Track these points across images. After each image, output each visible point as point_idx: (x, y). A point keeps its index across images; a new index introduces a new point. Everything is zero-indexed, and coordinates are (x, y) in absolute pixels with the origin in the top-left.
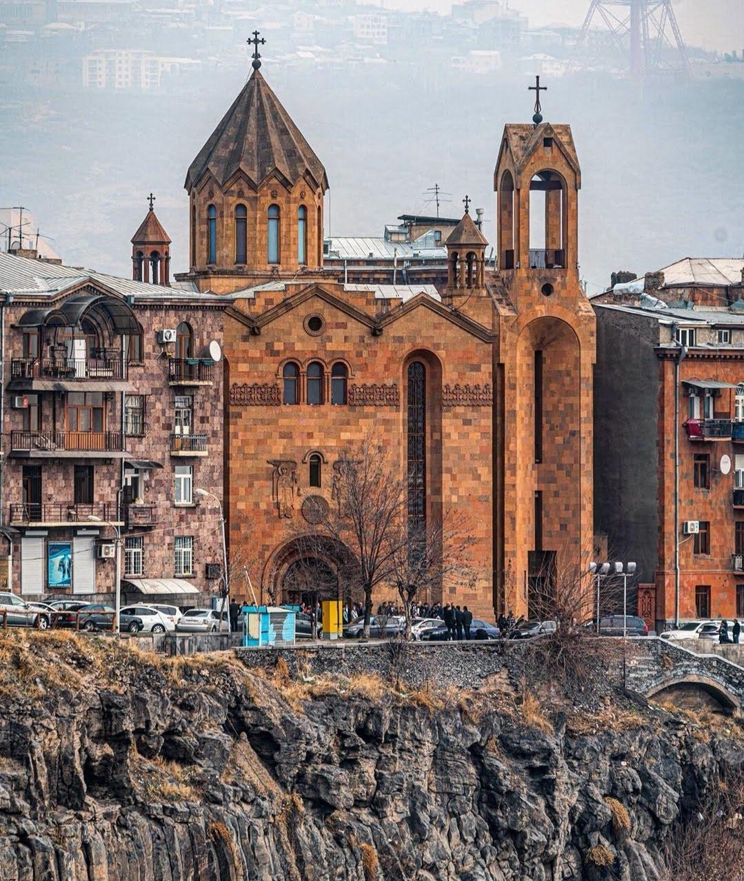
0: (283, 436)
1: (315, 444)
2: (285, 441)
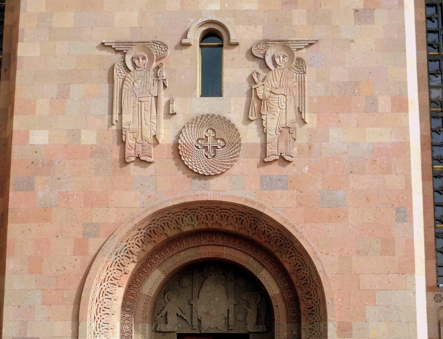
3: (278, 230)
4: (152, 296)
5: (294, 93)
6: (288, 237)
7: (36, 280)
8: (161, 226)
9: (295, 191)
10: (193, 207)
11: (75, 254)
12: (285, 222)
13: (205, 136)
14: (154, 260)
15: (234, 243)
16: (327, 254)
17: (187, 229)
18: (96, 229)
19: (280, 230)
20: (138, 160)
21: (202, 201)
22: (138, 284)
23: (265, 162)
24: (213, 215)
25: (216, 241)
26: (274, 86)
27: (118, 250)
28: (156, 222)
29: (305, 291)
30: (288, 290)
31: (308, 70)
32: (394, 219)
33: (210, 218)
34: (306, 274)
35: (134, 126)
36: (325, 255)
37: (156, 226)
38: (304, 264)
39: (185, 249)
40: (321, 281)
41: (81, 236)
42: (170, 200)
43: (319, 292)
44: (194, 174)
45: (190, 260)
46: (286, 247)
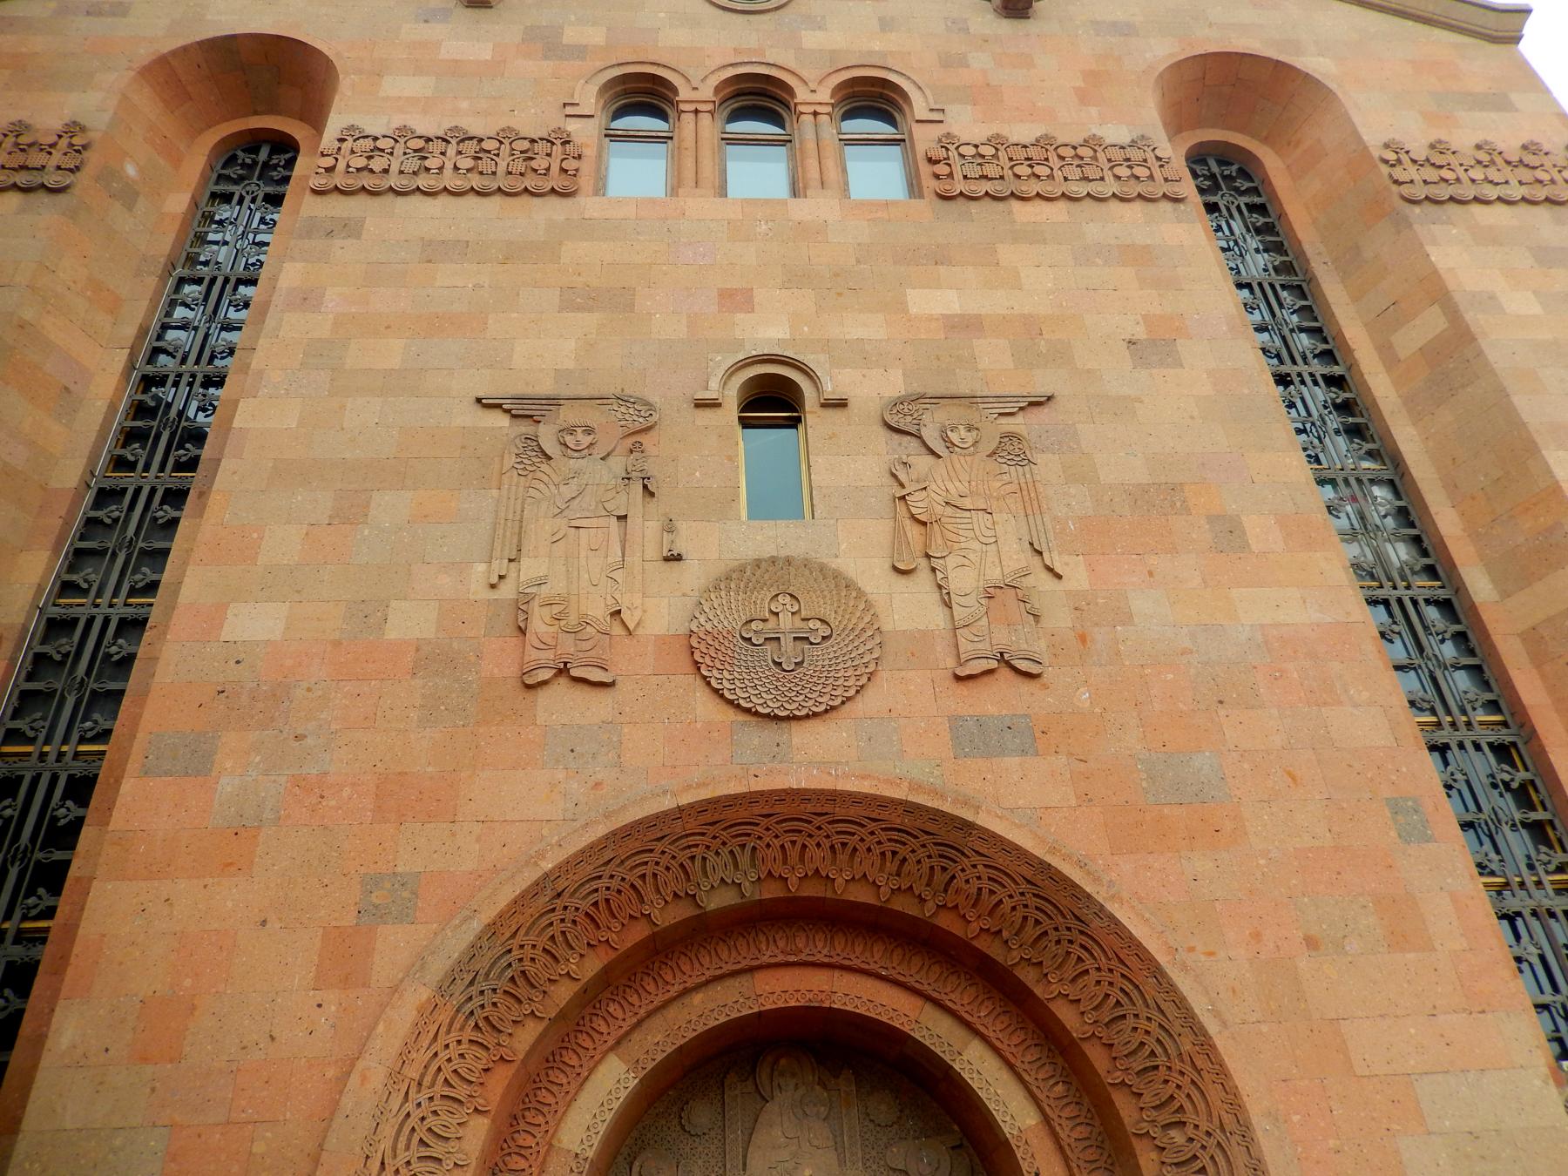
0: (577, 299)
1: (769, 331)
2: (590, 320)
3: (1029, 882)
4: (590, 1154)
5: (1013, 507)
6: (1065, 902)
7: (153, 1090)
8: (632, 886)
9: (1063, 759)
10: (743, 814)
11: (319, 983)
12: (1053, 850)
13: (771, 612)
14: (602, 1022)
15: (868, 954)
16: (1211, 954)
17: (719, 901)
18: (406, 894)
19: (1038, 879)
20: (563, 680)
21: (772, 792)
22: (545, 1110)
23: (958, 678)
24: (804, 846)
25: (807, 951)
26: (953, 491)
27: (482, 964)
28: (620, 872)
29: (1148, 1099)
30: (1068, 1109)
31: (1039, 458)
32: (1393, 834)
33: (793, 854)
34: (1147, 1032)
35: (556, 587)
36: (1203, 958)
37: (615, 884)
38: (1135, 994)
39: (707, 982)
40: (1213, 1047)
41: (349, 920)
42: (665, 792)
43: (1214, 1093)
44: (741, 717)
45: (722, 1019)
46: (1058, 942)
